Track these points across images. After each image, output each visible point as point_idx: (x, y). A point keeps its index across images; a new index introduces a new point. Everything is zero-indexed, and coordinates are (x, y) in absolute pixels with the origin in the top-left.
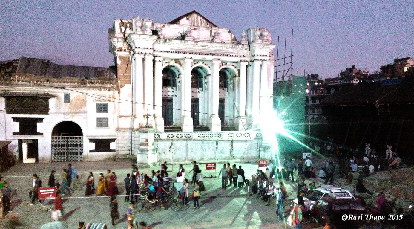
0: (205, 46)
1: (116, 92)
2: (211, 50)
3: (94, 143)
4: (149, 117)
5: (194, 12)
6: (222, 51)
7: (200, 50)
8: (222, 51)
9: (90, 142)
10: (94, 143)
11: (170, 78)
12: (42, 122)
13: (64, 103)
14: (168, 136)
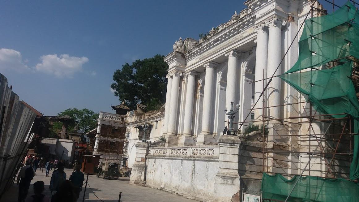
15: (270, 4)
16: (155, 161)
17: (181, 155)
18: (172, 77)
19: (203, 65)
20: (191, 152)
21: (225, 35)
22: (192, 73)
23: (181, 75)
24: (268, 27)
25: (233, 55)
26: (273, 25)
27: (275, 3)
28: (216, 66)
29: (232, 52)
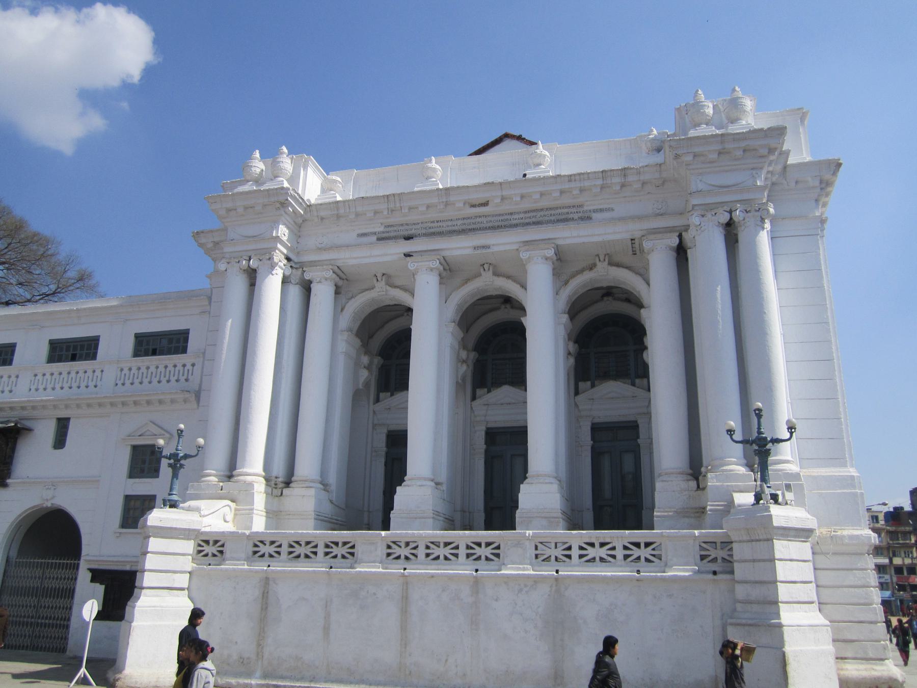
0: (485, 204)
2: (511, 214)
3: (103, 587)
6: (557, 208)
7: (469, 221)
8: (557, 208)
9: (93, 580)
10: (103, 587)
14: (256, 549)
22: (334, 276)
28: (444, 274)
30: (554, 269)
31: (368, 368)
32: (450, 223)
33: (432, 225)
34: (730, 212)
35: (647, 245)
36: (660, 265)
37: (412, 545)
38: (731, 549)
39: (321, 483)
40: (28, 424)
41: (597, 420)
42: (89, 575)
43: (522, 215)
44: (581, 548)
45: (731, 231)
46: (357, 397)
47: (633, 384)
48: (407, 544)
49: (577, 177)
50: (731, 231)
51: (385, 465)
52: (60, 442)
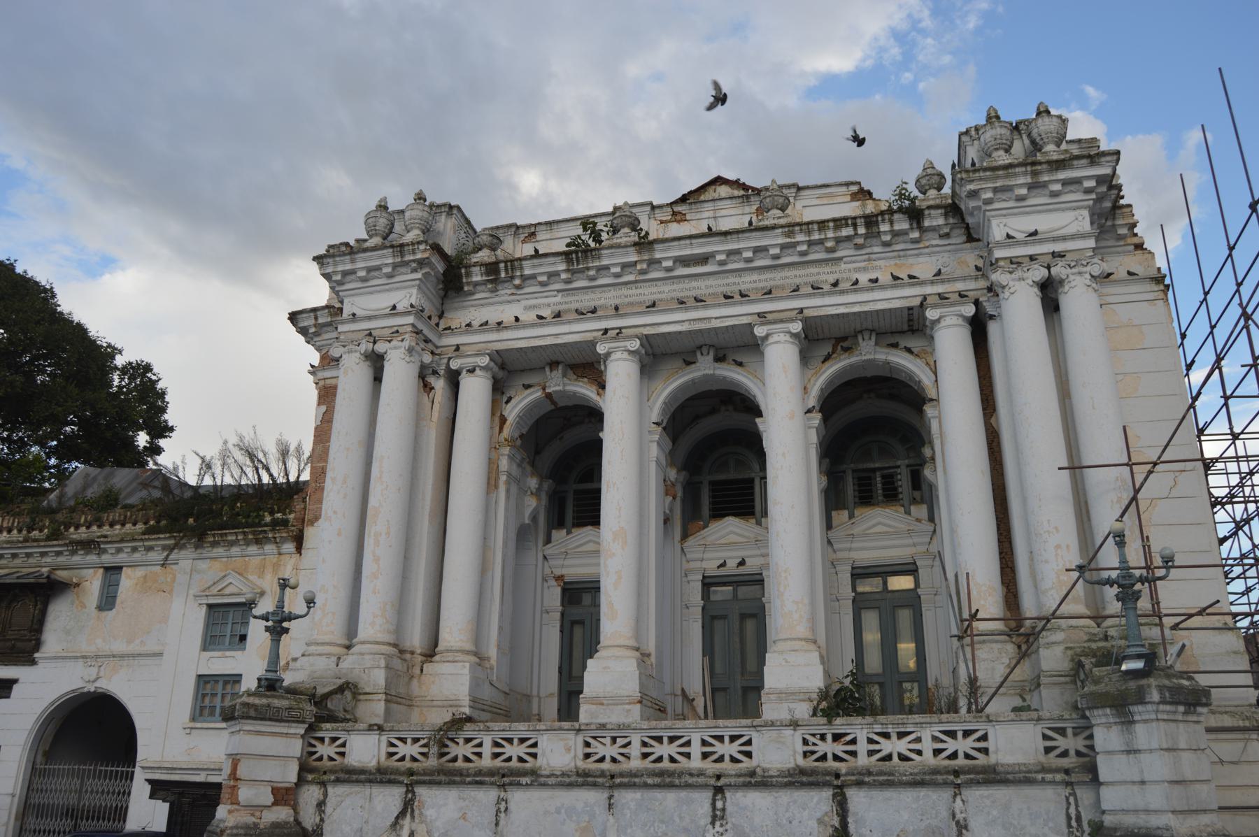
0: (704, 259)
1: (289, 547)
4: (286, 631)
5: (719, 181)
10: (167, 805)
11: (559, 463)
12: (8, 697)
13: (95, 612)
14: (392, 750)
15: (1063, 210)
16: (408, 807)
17: (696, 763)
18: (376, 362)
19: (593, 344)
20: (795, 752)
21: (757, 250)
22: (492, 364)
23: (427, 358)
24: (1061, 282)
25: (795, 335)
26: (1089, 283)
27: (1086, 213)
29: (797, 327)
30: (801, 352)
31: (537, 494)
32: (654, 290)
33: (630, 292)
34: (1049, 268)
35: (931, 314)
36: (952, 342)
37: (620, 742)
38: (1091, 737)
39: (476, 654)
40: (62, 575)
41: (857, 564)
42: (148, 788)
43: (755, 277)
44: (870, 741)
45: (1050, 294)
46: (523, 535)
47: (908, 513)
48: (614, 740)
49: (831, 224)
50: (1050, 294)
51: (561, 631)
52: (108, 601)
